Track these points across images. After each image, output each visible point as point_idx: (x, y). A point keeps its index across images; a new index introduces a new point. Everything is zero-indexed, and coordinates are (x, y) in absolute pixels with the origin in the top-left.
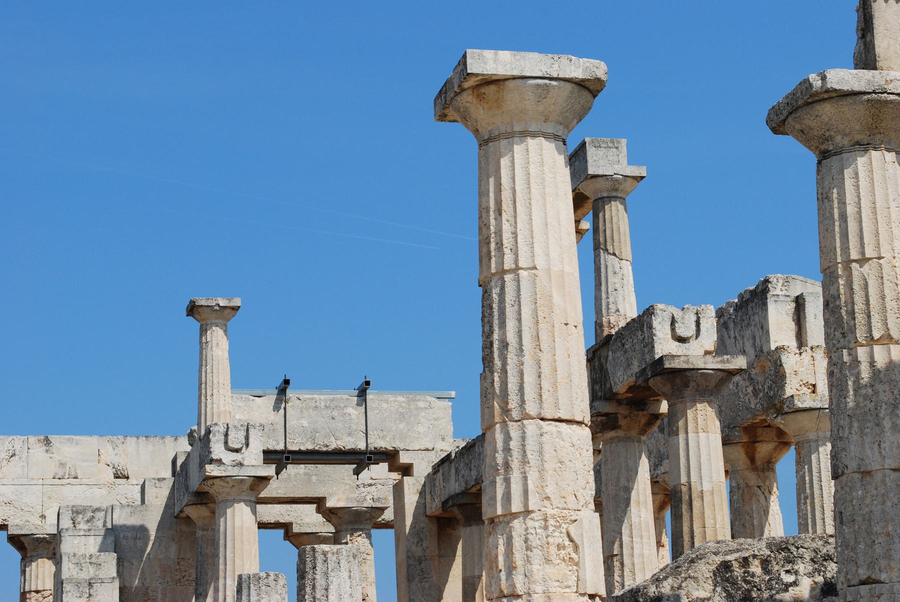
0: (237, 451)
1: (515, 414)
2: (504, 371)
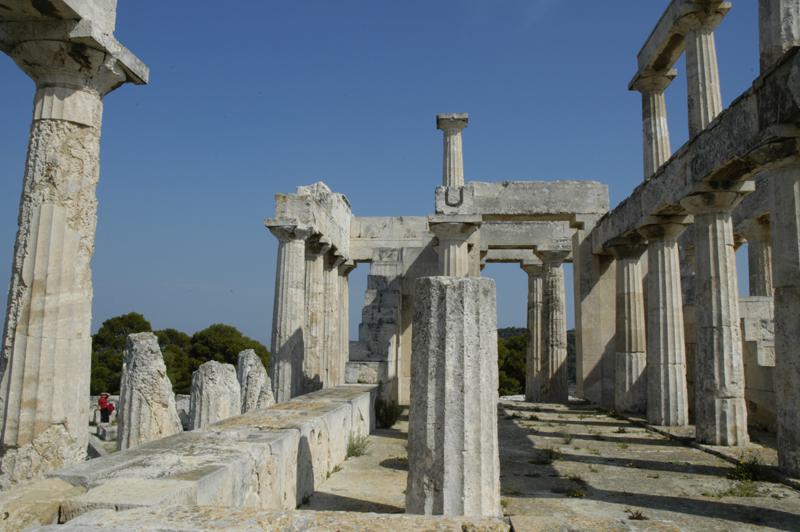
0: (454, 205)
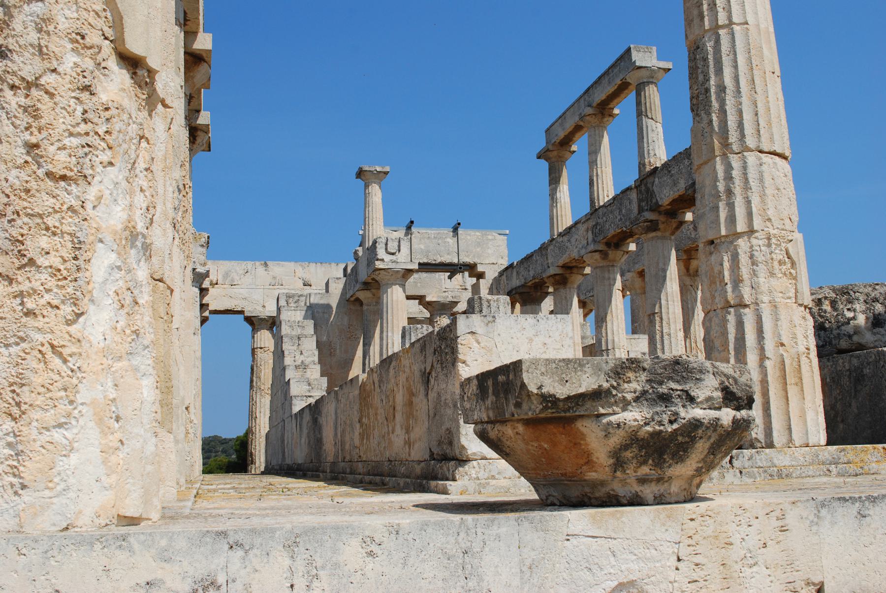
0: (393, 254)
1: (735, 147)
2: (723, 112)
